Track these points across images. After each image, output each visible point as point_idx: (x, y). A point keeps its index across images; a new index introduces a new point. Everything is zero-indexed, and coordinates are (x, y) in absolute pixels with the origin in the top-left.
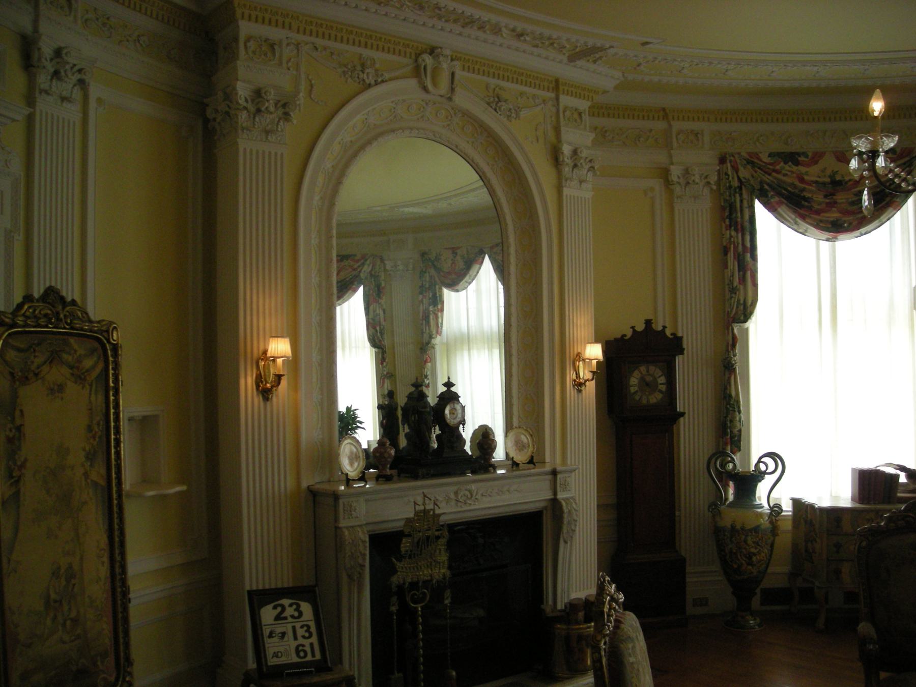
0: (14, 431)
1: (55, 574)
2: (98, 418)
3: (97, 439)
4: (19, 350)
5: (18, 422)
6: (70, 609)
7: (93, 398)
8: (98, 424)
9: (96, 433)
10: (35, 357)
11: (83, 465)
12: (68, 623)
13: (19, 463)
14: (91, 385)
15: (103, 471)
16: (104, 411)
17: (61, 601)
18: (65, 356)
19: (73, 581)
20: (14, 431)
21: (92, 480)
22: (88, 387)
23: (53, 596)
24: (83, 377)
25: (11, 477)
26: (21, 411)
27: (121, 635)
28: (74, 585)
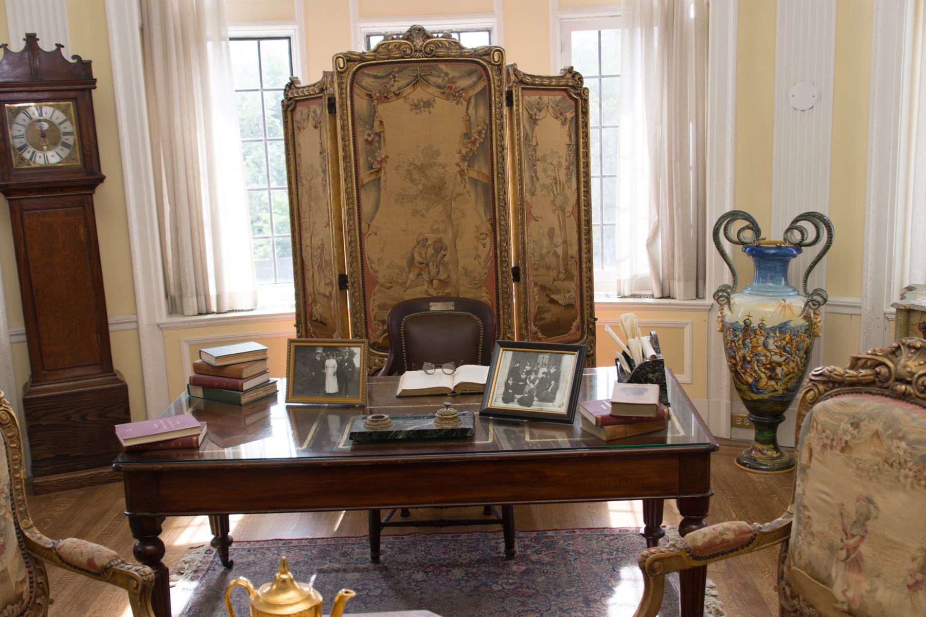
0: (372, 136)
1: (422, 243)
2: (479, 128)
3: (478, 145)
4: (375, 77)
5: (377, 129)
6: (439, 272)
7: (472, 111)
8: (480, 133)
9: (475, 139)
10: (395, 81)
11: (458, 165)
12: (435, 282)
13: (379, 159)
14: (469, 102)
15: (485, 170)
16: (487, 121)
17: (427, 265)
18: (433, 79)
19: (443, 252)
20: (372, 136)
21: (470, 178)
22: (465, 103)
23: (417, 258)
24: (457, 94)
25: (371, 168)
26: (381, 122)
28: (444, 255)
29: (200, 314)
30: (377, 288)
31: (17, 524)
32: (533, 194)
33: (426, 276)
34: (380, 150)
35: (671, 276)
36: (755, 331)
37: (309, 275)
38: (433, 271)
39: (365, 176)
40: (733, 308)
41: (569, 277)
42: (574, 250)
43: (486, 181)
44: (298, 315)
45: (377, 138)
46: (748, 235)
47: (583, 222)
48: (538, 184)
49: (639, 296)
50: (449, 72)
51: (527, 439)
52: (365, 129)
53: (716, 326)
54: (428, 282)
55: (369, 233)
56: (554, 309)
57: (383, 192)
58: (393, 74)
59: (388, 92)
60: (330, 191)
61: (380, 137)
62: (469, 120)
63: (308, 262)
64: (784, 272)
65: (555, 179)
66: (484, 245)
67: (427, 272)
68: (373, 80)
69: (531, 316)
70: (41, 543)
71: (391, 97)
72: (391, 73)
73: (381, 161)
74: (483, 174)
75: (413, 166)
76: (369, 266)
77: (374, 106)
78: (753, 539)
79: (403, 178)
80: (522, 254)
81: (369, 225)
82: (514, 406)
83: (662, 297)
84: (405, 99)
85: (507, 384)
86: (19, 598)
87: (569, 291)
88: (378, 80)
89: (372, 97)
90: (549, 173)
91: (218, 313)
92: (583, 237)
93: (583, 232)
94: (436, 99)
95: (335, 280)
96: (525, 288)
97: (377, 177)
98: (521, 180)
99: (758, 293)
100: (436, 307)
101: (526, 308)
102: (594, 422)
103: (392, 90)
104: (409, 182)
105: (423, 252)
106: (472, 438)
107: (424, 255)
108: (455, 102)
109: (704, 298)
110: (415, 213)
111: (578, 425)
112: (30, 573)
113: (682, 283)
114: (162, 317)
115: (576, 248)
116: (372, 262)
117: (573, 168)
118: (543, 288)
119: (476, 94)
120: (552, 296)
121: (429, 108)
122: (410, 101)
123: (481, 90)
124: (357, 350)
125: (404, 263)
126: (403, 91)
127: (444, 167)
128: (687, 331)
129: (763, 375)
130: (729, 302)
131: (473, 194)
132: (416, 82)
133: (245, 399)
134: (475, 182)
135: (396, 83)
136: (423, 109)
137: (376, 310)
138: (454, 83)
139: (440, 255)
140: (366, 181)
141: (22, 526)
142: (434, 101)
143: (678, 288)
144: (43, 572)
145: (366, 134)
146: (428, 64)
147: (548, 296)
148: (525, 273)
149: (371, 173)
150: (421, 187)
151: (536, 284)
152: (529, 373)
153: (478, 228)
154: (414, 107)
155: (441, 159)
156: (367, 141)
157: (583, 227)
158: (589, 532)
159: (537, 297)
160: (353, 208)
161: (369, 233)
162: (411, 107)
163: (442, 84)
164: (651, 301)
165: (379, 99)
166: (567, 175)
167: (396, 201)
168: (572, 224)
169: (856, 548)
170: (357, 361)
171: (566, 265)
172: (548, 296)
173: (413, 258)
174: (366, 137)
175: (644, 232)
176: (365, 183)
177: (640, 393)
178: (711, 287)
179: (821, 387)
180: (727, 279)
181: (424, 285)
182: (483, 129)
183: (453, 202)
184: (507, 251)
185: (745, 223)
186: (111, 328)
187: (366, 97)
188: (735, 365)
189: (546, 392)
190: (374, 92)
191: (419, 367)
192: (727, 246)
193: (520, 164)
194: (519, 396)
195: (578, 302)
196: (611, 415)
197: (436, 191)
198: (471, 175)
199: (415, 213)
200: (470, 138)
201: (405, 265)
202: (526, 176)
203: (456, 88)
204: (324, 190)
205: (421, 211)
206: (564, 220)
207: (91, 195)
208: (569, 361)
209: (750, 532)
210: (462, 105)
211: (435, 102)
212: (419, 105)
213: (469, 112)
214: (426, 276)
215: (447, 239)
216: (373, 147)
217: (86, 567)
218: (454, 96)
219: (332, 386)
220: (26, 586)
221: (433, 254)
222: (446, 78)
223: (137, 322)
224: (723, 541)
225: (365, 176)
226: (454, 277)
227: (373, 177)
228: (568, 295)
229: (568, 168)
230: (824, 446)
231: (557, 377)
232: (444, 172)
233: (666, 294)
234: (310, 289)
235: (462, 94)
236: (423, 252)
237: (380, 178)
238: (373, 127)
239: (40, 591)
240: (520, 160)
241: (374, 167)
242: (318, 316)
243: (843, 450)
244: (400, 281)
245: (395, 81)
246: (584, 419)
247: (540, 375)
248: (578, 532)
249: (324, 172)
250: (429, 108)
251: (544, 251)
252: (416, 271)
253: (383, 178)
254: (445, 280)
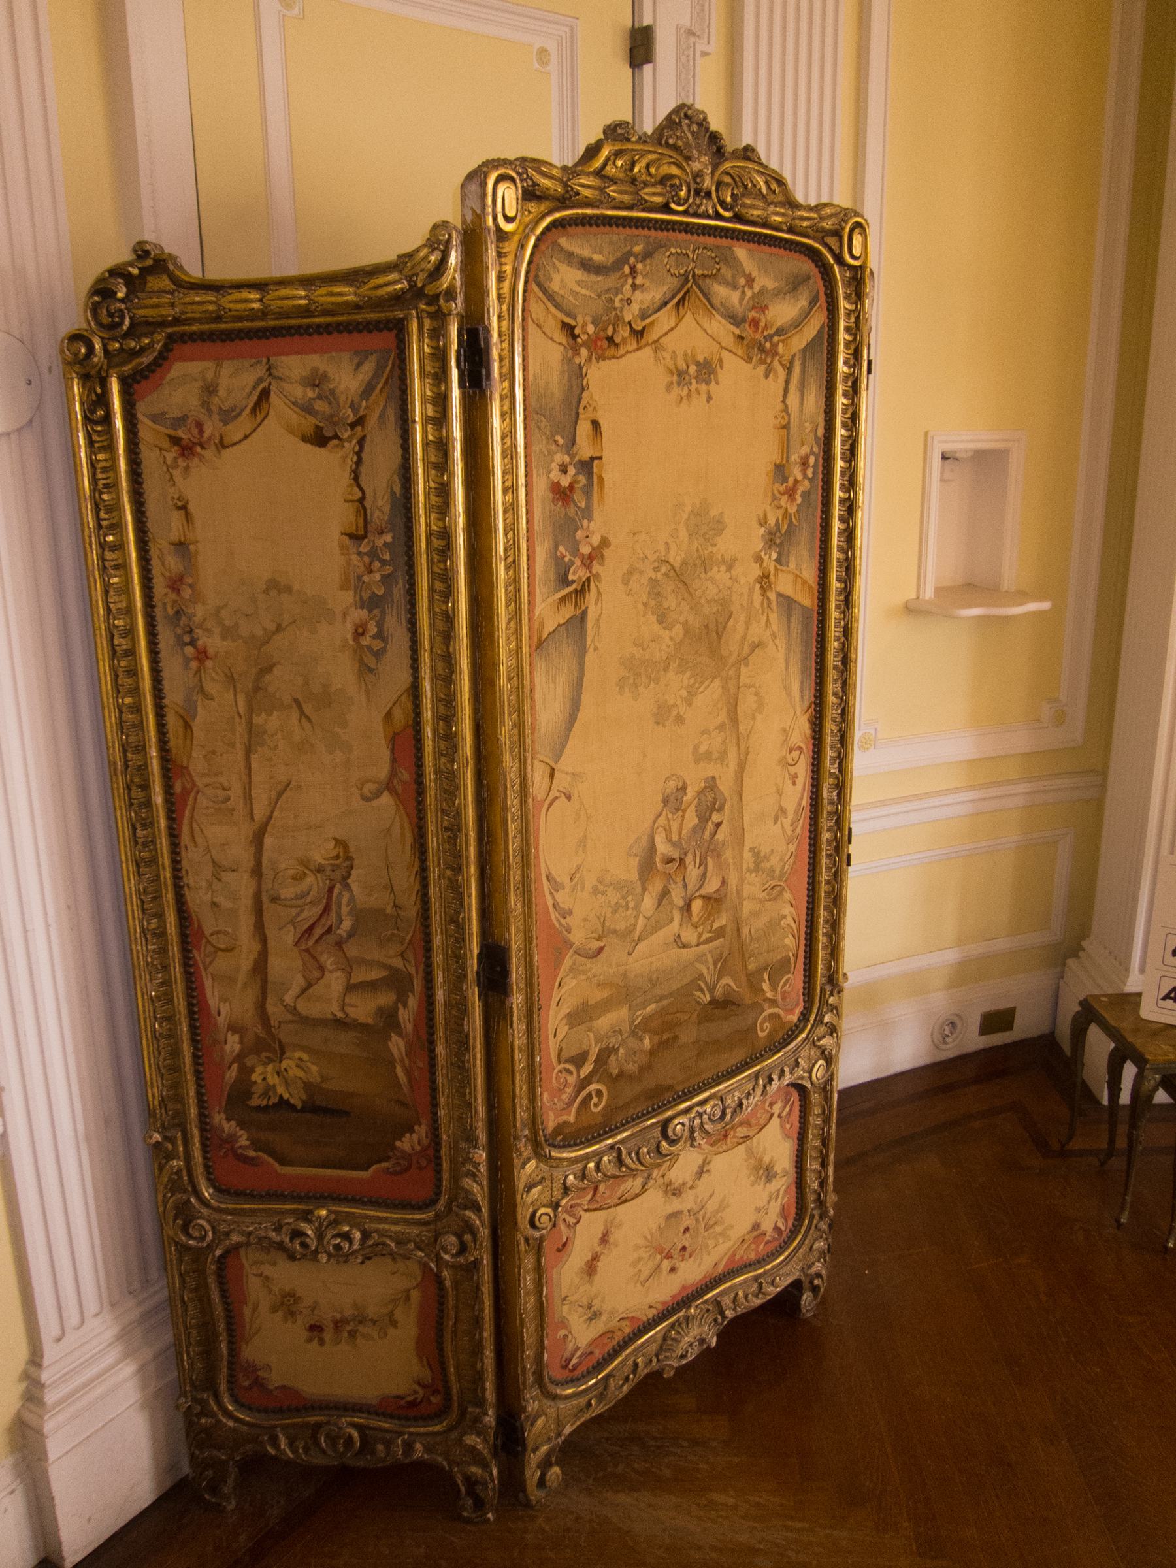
0: (572, 471)
1: (673, 801)
2: (805, 450)
3: (799, 500)
4: (587, 266)
5: (585, 450)
6: (704, 875)
7: (793, 400)
8: (804, 463)
9: (796, 481)
10: (634, 287)
11: (759, 559)
12: (697, 905)
13: (585, 550)
14: (789, 370)
15: (810, 574)
16: (821, 432)
17: (682, 860)
18: (720, 291)
19: (715, 817)
20: (572, 471)
21: (779, 595)
22: (782, 373)
23: (662, 848)
24: (768, 345)
25: (564, 581)
26: (595, 424)
27: (822, 929)
28: (718, 825)
34: (590, 518)
38: (693, 872)
45: (582, 479)
50: (755, 274)
52: (553, 447)
54: (681, 909)
55: (551, 797)
57: (590, 657)
58: (632, 260)
59: (617, 321)
61: (590, 475)
62: (786, 427)
67: (680, 884)
68: (579, 275)
71: (624, 339)
72: (623, 260)
73: (591, 557)
74: (804, 582)
75: (664, 569)
76: (550, 902)
77: (580, 367)
79: (640, 607)
81: (553, 770)
84: (656, 350)
88: (594, 278)
89: (575, 337)
94: (725, 354)
97: (579, 612)
103: (627, 319)
104: (654, 618)
105: (675, 827)
107: (675, 838)
108: (763, 367)
110: (662, 714)
116: (557, 886)
119: (805, 350)
121: (708, 383)
122: (667, 355)
123: (813, 339)
125: (629, 871)
126: (652, 323)
127: (730, 568)
131: (781, 642)
132: (683, 298)
135: (638, 295)
136: (694, 385)
137: (563, 1030)
138: (763, 309)
140: (550, 627)
142: (720, 361)
145: (555, 466)
146: (709, 241)
149: (563, 600)
154: (675, 378)
155: (726, 545)
156: (556, 488)
161: (551, 797)
162: (668, 379)
163: (740, 310)
165: (592, 344)
167: (621, 683)
173: (652, 848)
174: (555, 475)
176: (545, 635)
181: (672, 920)
182: (812, 452)
183: (743, 670)
187: (560, 337)
190: (580, 318)
199: (662, 714)
200: (785, 480)
201: (634, 876)
203: (766, 327)
205: (675, 705)
210: (776, 376)
211: (721, 368)
212: (687, 372)
213: (788, 402)
215: (725, 786)
216: (571, 511)
218: (761, 349)
221: (694, 829)
222: (749, 293)
226: (733, 881)
227: (568, 611)
232: (729, 583)
235: (777, 345)
236: (675, 827)
237: (584, 613)
238: (574, 442)
241: (571, 577)
244: (621, 926)
245: (634, 287)
250: (708, 383)
252: (657, 886)
254: (716, 896)
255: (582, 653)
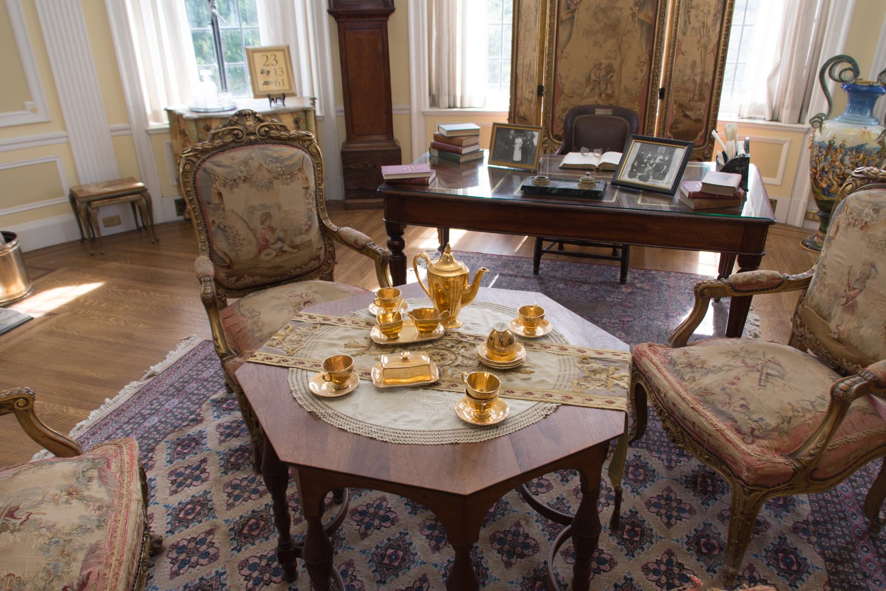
1: (598, 66)
6: (607, 88)
11: (631, 9)
12: (603, 95)
15: (651, 14)
17: (599, 83)
19: (611, 74)
23: (593, 77)
25: (569, 8)
28: (612, 76)
29: (449, 107)
30: (563, 96)
31: (318, 215)
32: (684, 34)
33: (597, 91)
35: (781, 105)
36: (836, 150)
37: (519, 85)
38: (603, 87)
39: (564, 15)
40: (823, 131)
41: (702, 99)
42: (709, 80)
43: (650, 22)
44: (510, 113)
46: (848, 75)
47: (720, 58)
48: (689, 27)
49: (755, 119)
51: (639, 202)
53: (808, 144)
56: (687, 122)
57: (575, 27)
60: (538, 25)
63: (520, 77)
64: (872, 106)
65: (704, 23)
66: (642, 71)
69: (668, 125)
70: (331, 228)
74: (649, 17)
78: (780, 284)
80: (668, 78)
82: (636, 180)
83: (772, 120)
85: (633, 165)
86: (318, 258)
87: (700, 110)
90: (700, 18)
91: (461, 108)
92: (718, 69)
93: (719, 66)
95: (535, 89)
96: (667, 105)
98: (677, 22)
99: (847, 121)
100: (599, 112)
101: (665, 119)
102: (687, 195)
106: (601, 198)
109: (803, 123)
110: (596, 44)
111: (677, 197)
112: (325, 244)
113: (789, 111)
114: (427, 108)
115: (710, 77)
116: (561, 78)
117: (719, 15)
118: (681, 106)
120: (687, 112)
124: (536, 134)
125: (584, 81)
128: (785, 147)
129: (835, 183)
130: (821, 127)
133: (462, 160)
134: (642, 22)
137: (560, 112)
139: (609, 76)
140: (564, 18)
141: (321, 217)
143: (785, 114)
144: (332, 246)
147: (683, 111)
148: (668, 93)
150: (602, 24)
151: (675, 102)
152: (650, 159)
153: (639, 58)
157: (719, 62)
158: (680, 275)
159: (675, 112)
160: (553, 38)
164: (762, 122)
166: (713, 20)
168: (711, 59)
169: (854, 297)
170: (535, 141)
171: (701, 90)
172: (683, 111)
173: (590, 76)
175: (769, 69)
177: (726, 179)
178: (811, 113)
179: (859, 182)
180: (825, 110)
183: (624, 38)
184: (658, 76)
185: (848, 65)
186: (394, 112)
188: (815, 174)
189: (660, 173)
191: (577, 150)
192: (830, 84)
193: (678, 10)
194: (639, 174)
195: (706, 118)
196: (700, 192)
197: (613, 29)
198: (640, 17)
199: (596, 44)
202: (681, 19)
204: (535, 24)
206: (705, 56)
207: (386, 21)
208: (680, 153)
209: (780, 278)
214: (597, 91)
215: (616, 66)
217: (353, 244)
219: (517, 156)
220: (323, 252)
221: (604, 75)
223: (410, 109)
224: (758, 282)
225: (564, 15)
226: (617, 92)
227: (570, 15)
228: (698, 113)
229: (715, 15)
230: (849, 224)
231: (669, 163)
233: (776, 118)
234: (519, 96)
239: (330, 256)
240: (678, 7)
242: (522, 114)
243: (862, 228)
246: (682, 193)
247: (657, 161)
248: (672, 274)
249: (536, 10)
251: (686, 78)
252: (591, 87)
253: (576, 17)
255: (572, 25)
